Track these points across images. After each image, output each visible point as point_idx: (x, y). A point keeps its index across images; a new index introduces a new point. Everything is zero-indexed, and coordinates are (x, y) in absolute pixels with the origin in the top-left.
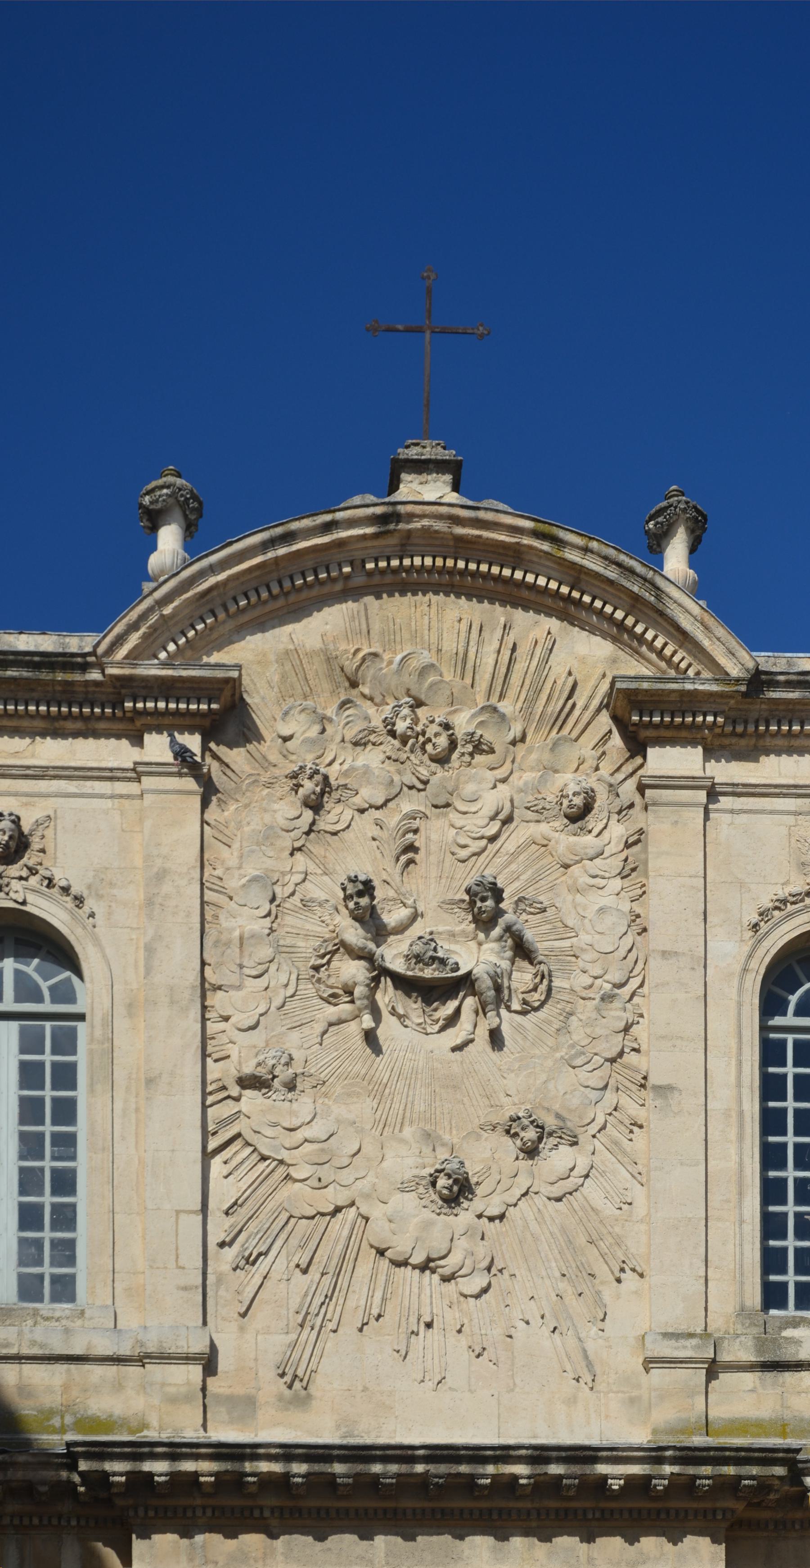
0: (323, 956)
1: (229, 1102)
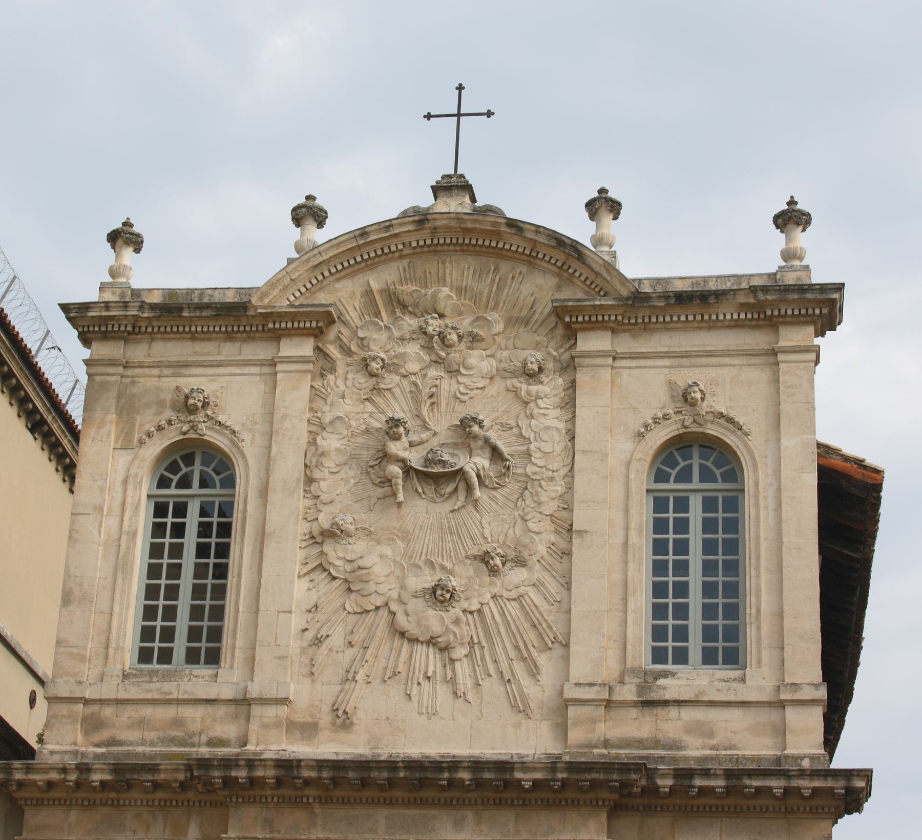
0: (377, 459)
1: (317, 546)
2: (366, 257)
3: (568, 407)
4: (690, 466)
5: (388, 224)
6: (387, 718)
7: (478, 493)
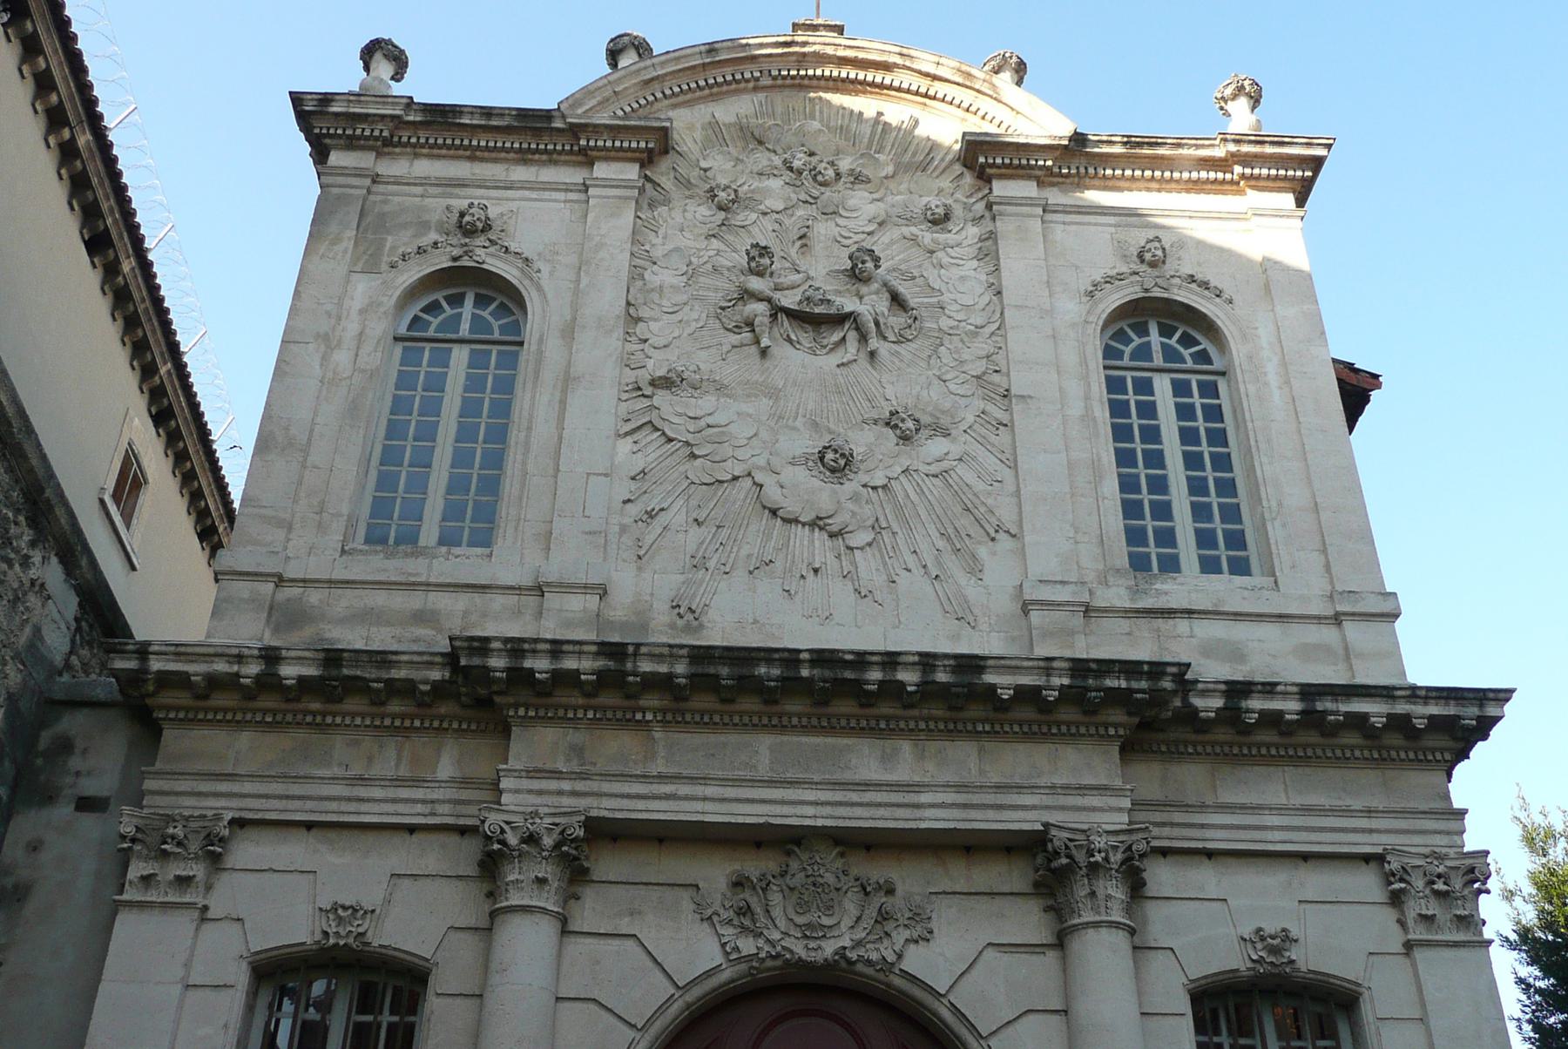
0: (730, 301)
1: (644, 400)
2: (711, 81)
3: (988, 259)
4: (1149, 343)
6: (755, 622)
7: (874, 343)
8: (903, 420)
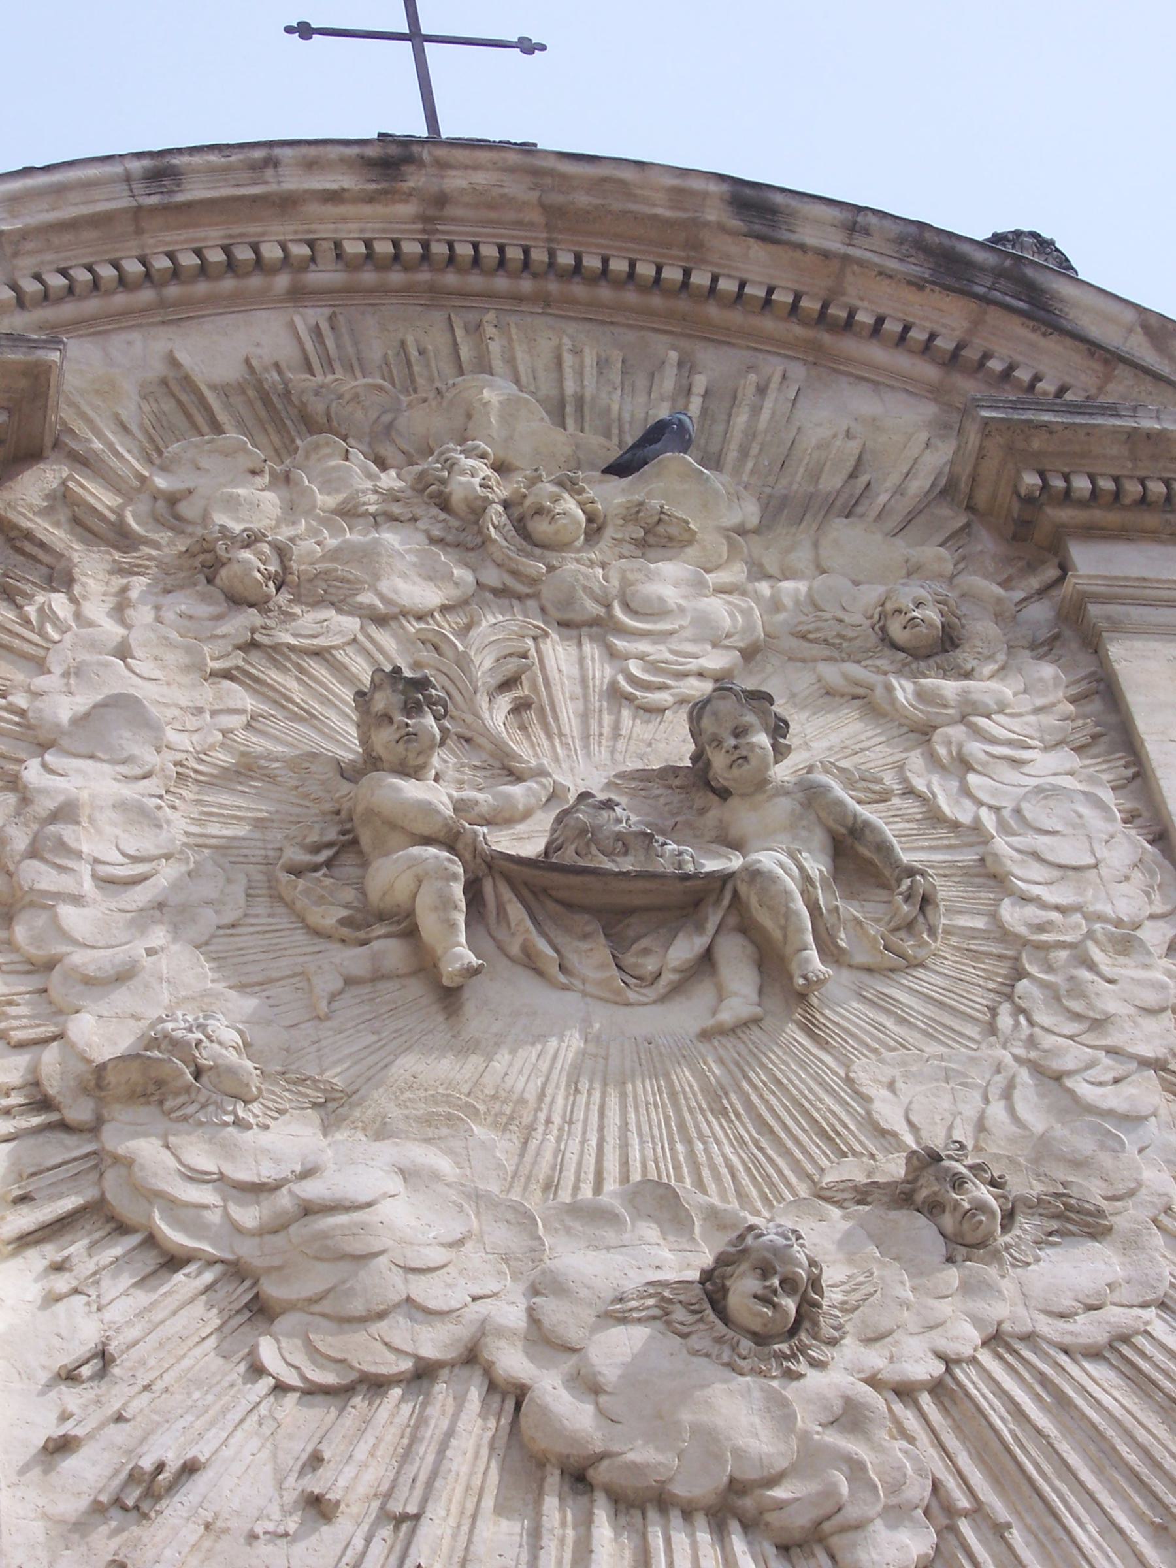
0: (316, 849)
5: (258, 154)
8: (958, 1183)
